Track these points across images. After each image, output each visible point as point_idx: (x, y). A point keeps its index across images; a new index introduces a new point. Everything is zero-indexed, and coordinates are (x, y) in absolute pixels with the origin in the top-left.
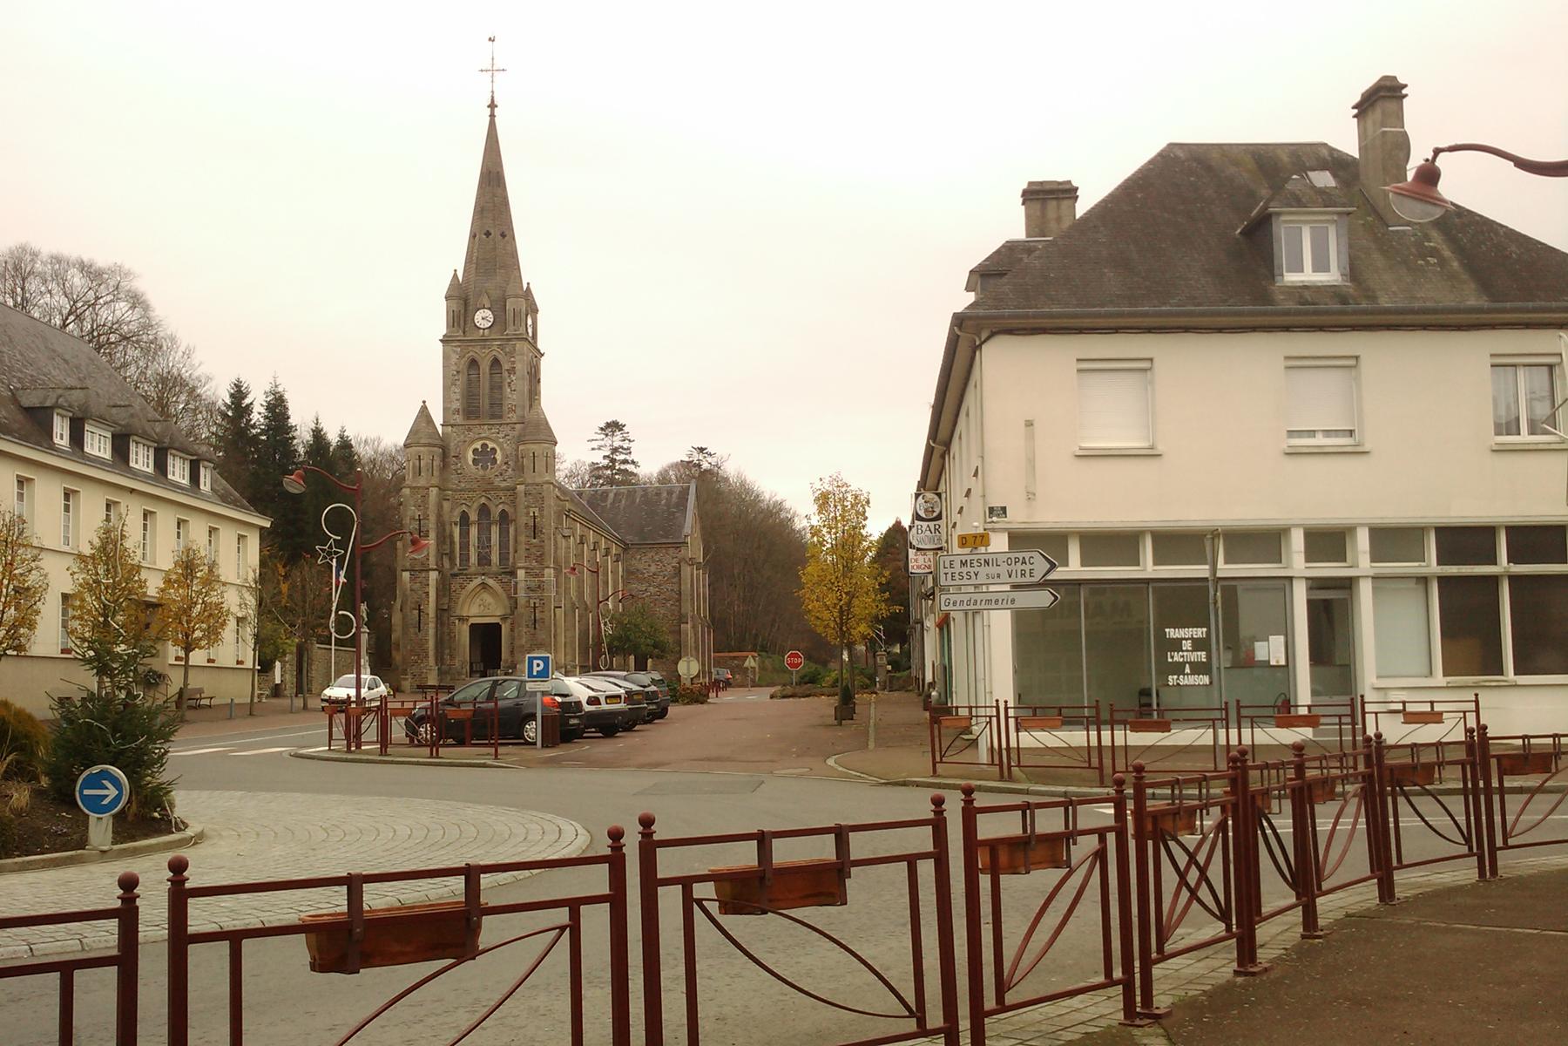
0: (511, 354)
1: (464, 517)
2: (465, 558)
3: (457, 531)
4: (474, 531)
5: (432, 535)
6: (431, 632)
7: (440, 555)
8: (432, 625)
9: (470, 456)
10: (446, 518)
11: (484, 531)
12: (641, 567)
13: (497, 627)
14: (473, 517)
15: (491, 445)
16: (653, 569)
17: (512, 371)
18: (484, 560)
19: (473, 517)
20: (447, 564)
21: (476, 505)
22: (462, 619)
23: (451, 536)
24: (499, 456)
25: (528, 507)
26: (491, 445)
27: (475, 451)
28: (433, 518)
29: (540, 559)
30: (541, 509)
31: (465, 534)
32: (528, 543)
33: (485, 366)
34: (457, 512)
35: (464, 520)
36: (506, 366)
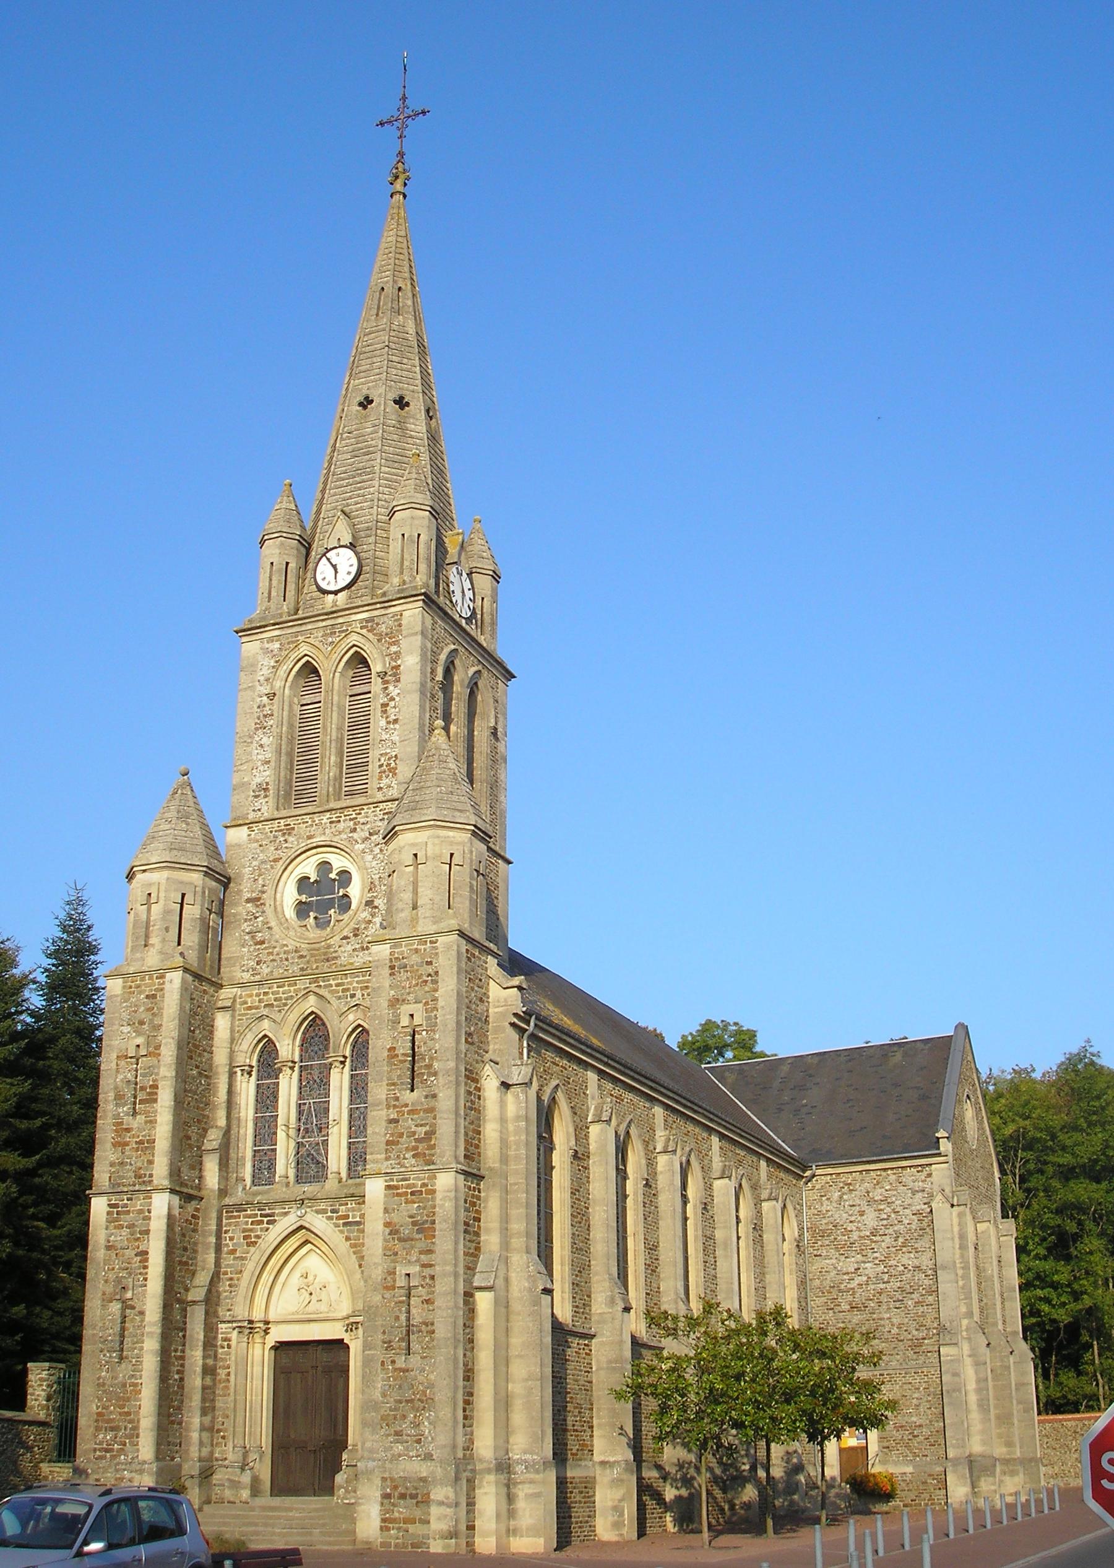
0: (391, 637)
1: (268, 1049)
2: (265, 1163)
3: (247, 1089)
4: (288, 1086)
5: (165, 1097)
9: (289, 895)
11: (314, 1084)
12: (841, 1216)
13: (339, 1345)
14: (288, 1048)
16: (870, 1219)
17: (392, 675)
18: (310, 1164)
19: (288, 1048)
21: (294, 1017)
22: (249, 1328)
24: (355, 891)
27: (303, 881)
31: (267, 1099)
32: (393, 1102)
34: (248, 1042)
36: (377, 667)
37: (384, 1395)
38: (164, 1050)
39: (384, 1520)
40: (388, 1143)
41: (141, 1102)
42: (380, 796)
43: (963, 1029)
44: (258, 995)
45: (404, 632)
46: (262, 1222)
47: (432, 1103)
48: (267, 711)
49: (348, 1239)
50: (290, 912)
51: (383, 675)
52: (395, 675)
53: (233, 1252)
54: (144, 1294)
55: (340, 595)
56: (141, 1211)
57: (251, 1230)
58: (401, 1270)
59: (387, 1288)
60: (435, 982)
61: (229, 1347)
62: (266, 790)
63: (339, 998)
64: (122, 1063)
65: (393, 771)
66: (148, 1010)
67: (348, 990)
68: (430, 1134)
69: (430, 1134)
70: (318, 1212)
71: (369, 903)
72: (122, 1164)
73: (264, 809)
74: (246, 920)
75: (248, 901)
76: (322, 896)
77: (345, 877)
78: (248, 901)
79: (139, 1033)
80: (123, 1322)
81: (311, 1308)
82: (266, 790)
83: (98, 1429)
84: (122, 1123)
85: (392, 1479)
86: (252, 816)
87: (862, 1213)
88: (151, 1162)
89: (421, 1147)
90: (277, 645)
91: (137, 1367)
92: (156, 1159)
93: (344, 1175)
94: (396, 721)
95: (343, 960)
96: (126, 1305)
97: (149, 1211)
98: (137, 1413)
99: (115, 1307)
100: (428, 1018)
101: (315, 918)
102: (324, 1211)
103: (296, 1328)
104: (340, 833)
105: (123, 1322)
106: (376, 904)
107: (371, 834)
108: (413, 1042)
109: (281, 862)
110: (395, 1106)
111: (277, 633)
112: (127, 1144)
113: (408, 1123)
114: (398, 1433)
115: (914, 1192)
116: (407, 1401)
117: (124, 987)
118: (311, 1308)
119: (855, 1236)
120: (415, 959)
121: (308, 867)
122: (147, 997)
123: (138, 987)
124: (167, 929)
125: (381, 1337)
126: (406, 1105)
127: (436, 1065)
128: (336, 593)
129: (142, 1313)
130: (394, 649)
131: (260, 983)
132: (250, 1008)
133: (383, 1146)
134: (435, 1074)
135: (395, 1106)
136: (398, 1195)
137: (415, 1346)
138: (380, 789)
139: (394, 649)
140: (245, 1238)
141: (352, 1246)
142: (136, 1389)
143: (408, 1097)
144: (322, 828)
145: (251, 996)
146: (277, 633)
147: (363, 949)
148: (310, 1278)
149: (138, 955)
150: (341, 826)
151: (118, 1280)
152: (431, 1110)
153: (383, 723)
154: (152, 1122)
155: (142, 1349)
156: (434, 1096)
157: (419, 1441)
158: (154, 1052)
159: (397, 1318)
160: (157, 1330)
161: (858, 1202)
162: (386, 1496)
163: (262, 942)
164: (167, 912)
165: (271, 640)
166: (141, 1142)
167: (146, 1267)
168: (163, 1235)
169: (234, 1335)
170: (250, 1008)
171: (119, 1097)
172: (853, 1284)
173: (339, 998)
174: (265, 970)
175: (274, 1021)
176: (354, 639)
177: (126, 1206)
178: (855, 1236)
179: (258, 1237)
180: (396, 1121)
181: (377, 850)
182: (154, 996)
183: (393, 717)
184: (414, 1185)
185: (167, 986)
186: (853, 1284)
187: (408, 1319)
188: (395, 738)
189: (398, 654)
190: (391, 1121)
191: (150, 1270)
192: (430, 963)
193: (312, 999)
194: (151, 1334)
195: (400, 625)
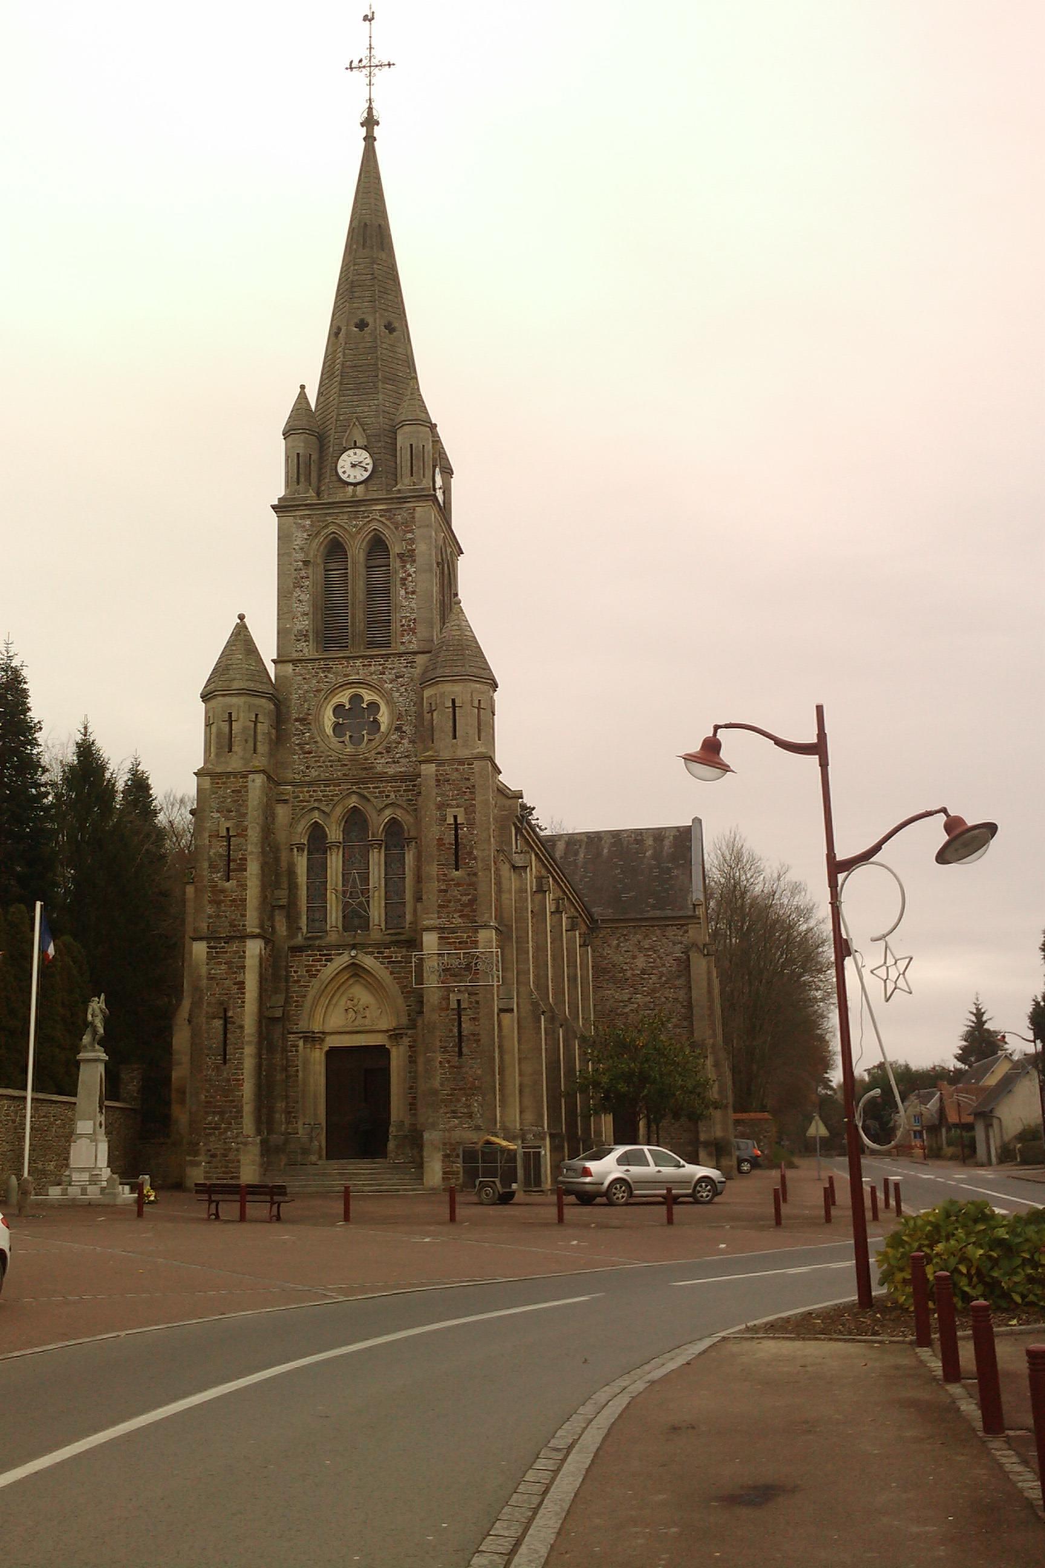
0: (408, 525)
1: (317, 833)
3: (301, 863)
5: (253, 868)
6: (249, 1064)
7: (268, 908)
8: (249, 1051)
9: (328, 719)
10: (282, 837)
11: (355, 862)
12: (618, 959)
13: (382, 1051)
14: (334, 833)
15: (368, 696)
16: (641, 962)
17: (407, 557)
19: (334, 833)
20: (282, 929)
21: (339, 811)
22: (313, 1038)
23: (291, 873)
24: (384, 717)
25: (441, 806)
26: (368, 696)
27: (338, 709)
28: (254, 834)
29: (470, 910)
30: (470, 810)
31: (317, 869)
32: (444, 878)
33: (357, 551)
34: (302, 827)
35: (317, 842)
36: (396, 549)
37: (442, 1085)
38: (250, 832)
39: (444, 1173)
40: (440, 906)
41: (235, 870)
42: (402, 649)
43: (697, 821)
44: (308, 792)
45: (417, 524)
46: (320, 960)
47: (474, 879)
48: (303, 573)
49: (392, 973)
50: (329, 731)
51: (400, 556)
52: (411, 556)
53: (298, 981)
54: (242, 1013)
55: (358, 487)
56: (237, 952)
57: (312, 966)
58: (453, 997)
59: (442, 1009)
60: (473, 793)
61: (297, 1051)
62: (305, 636)
63: (376, 797)
64: (214, 840)
65: (413, 631)
66: (235, 801)
67: (384, 792)
68: (472, 902)
69: (472, 902)
70: (366, 953)
71: (398, 729)
72: (218, 916)
73: (306, 650)
74: (295, 735)
75: (296, 720)
76: (356, 717)
77: (374, 706)
78: (296, 720)
79: (228, 819)
80: (225, 1034)
81: (356, 1023)
82: (305, 636)
83: (207, 1113)
84: (216, 886)
85: (451, 1144)
86: (295, 655)
87: (634, 957)
88: (244, 916)
89: (467, 910)
90: (308, 522)
91: (239, 1067)
92: (248, 913)
93: (383, 926)
94: (413, 593)
95: (379, 768)
96: (226, 1020)
97: (244, 952)
98: (241, 1101)
99: (218, 1023)
100: (467, 819)
101: (350, 737)
102: (372, 953)
103: (347, 1037)
104: (372, 674)
105: (225, 1034)
106: (404, 728)
107: (397, 677)
108: (456, 835)
109: (323, 692)
110: (444, 880)
111: (307, 512)
112: (223, 901)
113: (455, 892)
114: (453, 1112)
115: (674, 944)
116: (460, 1089)
117: (212, 783)
118: (356, 1023)
119: (629, 974)
120: (455, 775)
121: (343, 698)
122: (233, 791)
123: (224, 783)
124: (246, 741)
125: (438, 1044)
126: (453, 880)
127: (475, 852)
128: (355, 485)
129: (242, 1027)
130: (409, 536)
131: (310, 784)
132: (302, 801)
133: (435, 908)
134: (475, 859)
135: (444, 880)
136: (449, 943)
137: (465, 1050)
138: (403, 643)
139: (409, 536)
140: (307, 971)
141: (395, 978)
142: (239, 1083)
143: (457, 873)
144: (357, 670)
145: (302, 792)
146: (307, 512)
147: (394, 762)
148: (356, 1001)
149: (223, 759)
150: (373, 668)
151: (221, 1003)
152: (472, 884)
153: (403, 592)
154: (243, 886)
155: (242, 1053)
156: (475, 874)
157: (471, 1117)
158: (242, 833)
159: (451, 1031)
160: (254, 1039)
161: (631, 948)
162: (446, 1156)
163: (310, 753)
164: (245, 728)
165: (303, 517)
166: (234, 900)
167: (243, 993)
168: (256, 970)
169: (301, 1043)
170: (302, 801)
171: (212, 867)
172: (627, 1010)
173: (376, 797)
174: (314, 773)
175: (324, 812)
176: (374, 525)
177: (223, 947)
178: (629, 974)
179: (318, 971)
180: (446, 891)
181: (403, 689)
182: (239, 791)
183: (410, 589)
184: (462, 937)
185: (250, 784)
186: (627, 1010)
187: (460, 1032)
188: (413, 605)
189: (412, 541)
190: (441, 891)
191: (247, 995)
192: (468, 779)
193: (354, 798)
194: (249, 1043)
195: (413, 518)
